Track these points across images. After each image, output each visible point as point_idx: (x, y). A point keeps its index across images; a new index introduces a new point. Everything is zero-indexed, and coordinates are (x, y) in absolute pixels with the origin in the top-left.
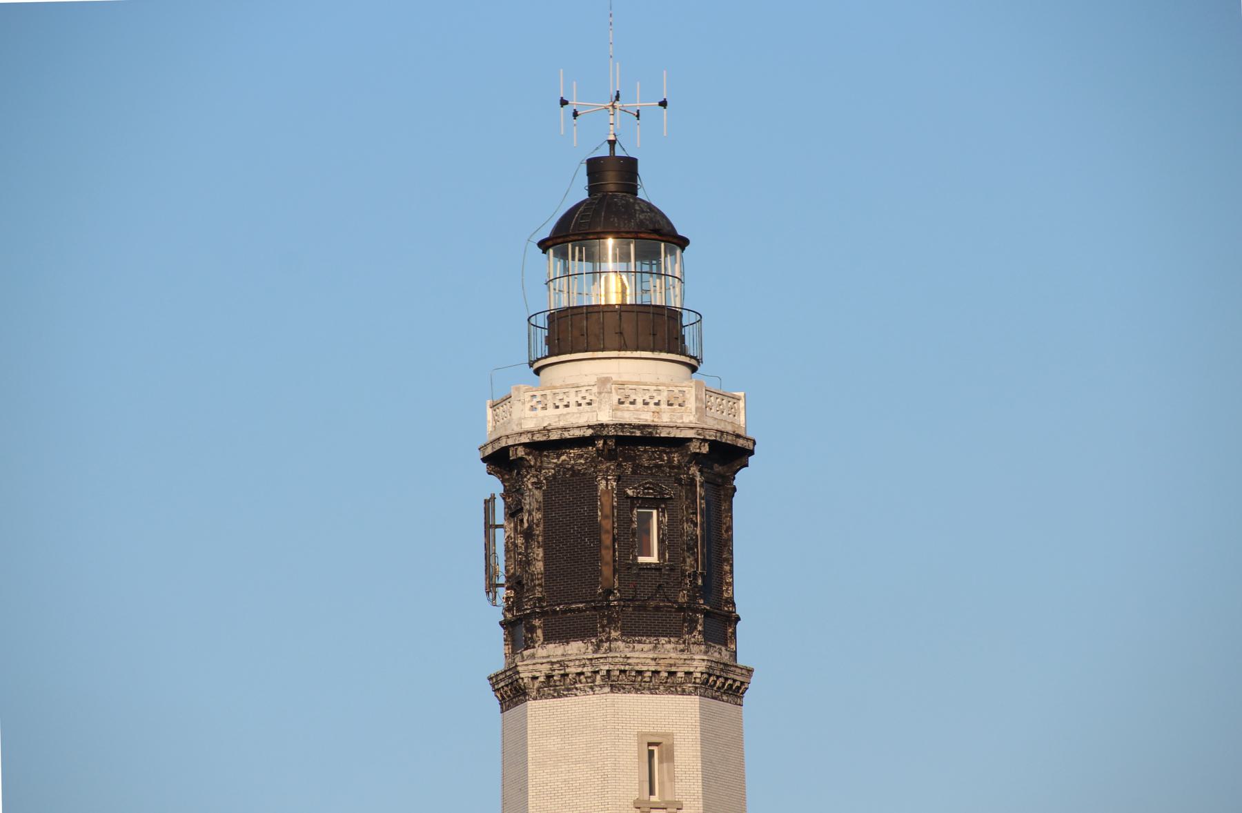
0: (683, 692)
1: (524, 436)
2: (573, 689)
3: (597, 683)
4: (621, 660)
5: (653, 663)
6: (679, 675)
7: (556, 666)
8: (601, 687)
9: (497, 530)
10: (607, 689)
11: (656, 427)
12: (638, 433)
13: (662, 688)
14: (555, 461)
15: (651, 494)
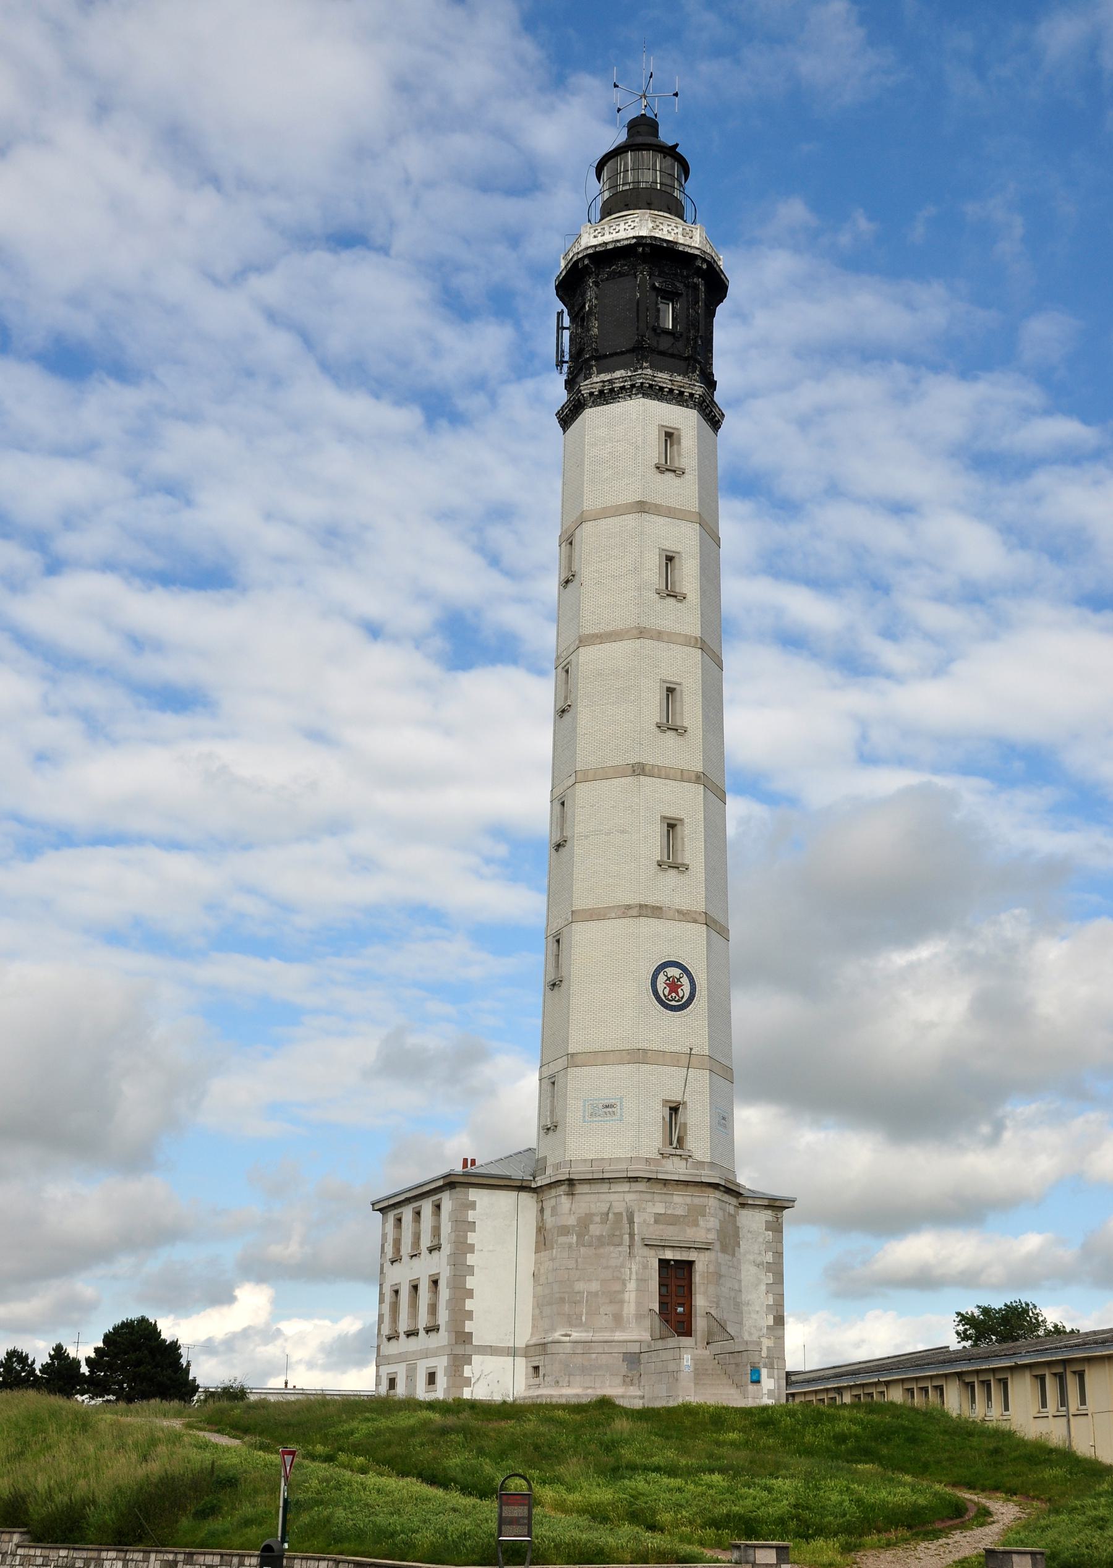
0: (687, 407)
1: (589, 250)
2: (616, 398)
3: (634, 393)
4: (650, 377)
6: (686, 394)
8: (636, 394)
9: (564, 331)
10: (641, 396)
11: (676, 243)
12: (665, 245)
13: (674, 401)
14: (608, 270)
15: (670, 288)
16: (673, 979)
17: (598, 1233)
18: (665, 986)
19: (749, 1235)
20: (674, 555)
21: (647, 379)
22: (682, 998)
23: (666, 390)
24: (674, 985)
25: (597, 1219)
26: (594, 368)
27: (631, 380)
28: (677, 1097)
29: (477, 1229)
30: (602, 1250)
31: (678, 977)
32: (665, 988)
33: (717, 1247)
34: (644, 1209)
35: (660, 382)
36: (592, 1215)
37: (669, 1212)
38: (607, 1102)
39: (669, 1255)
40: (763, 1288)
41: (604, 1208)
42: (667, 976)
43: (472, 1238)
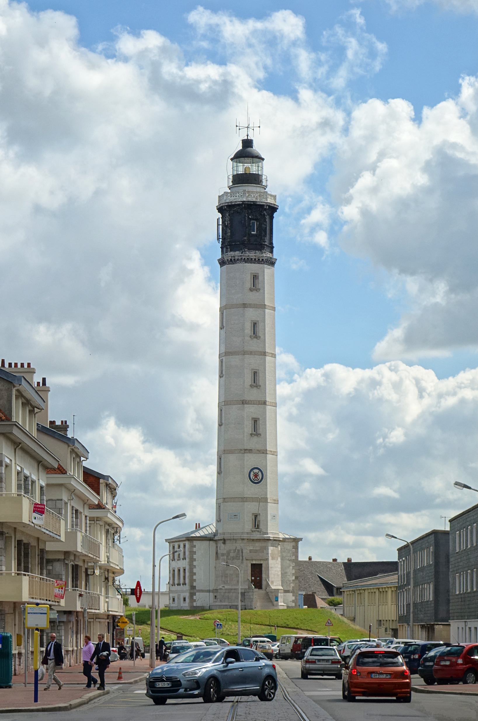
8: (243, 262)
10: (244, 262)
12: (252, 203)
17: (232, 556)
24: (256, 475)
25: (232, 551)
36: (231, 550)
37: (254, 549)
38: (235, 514)
39: (254, 562)
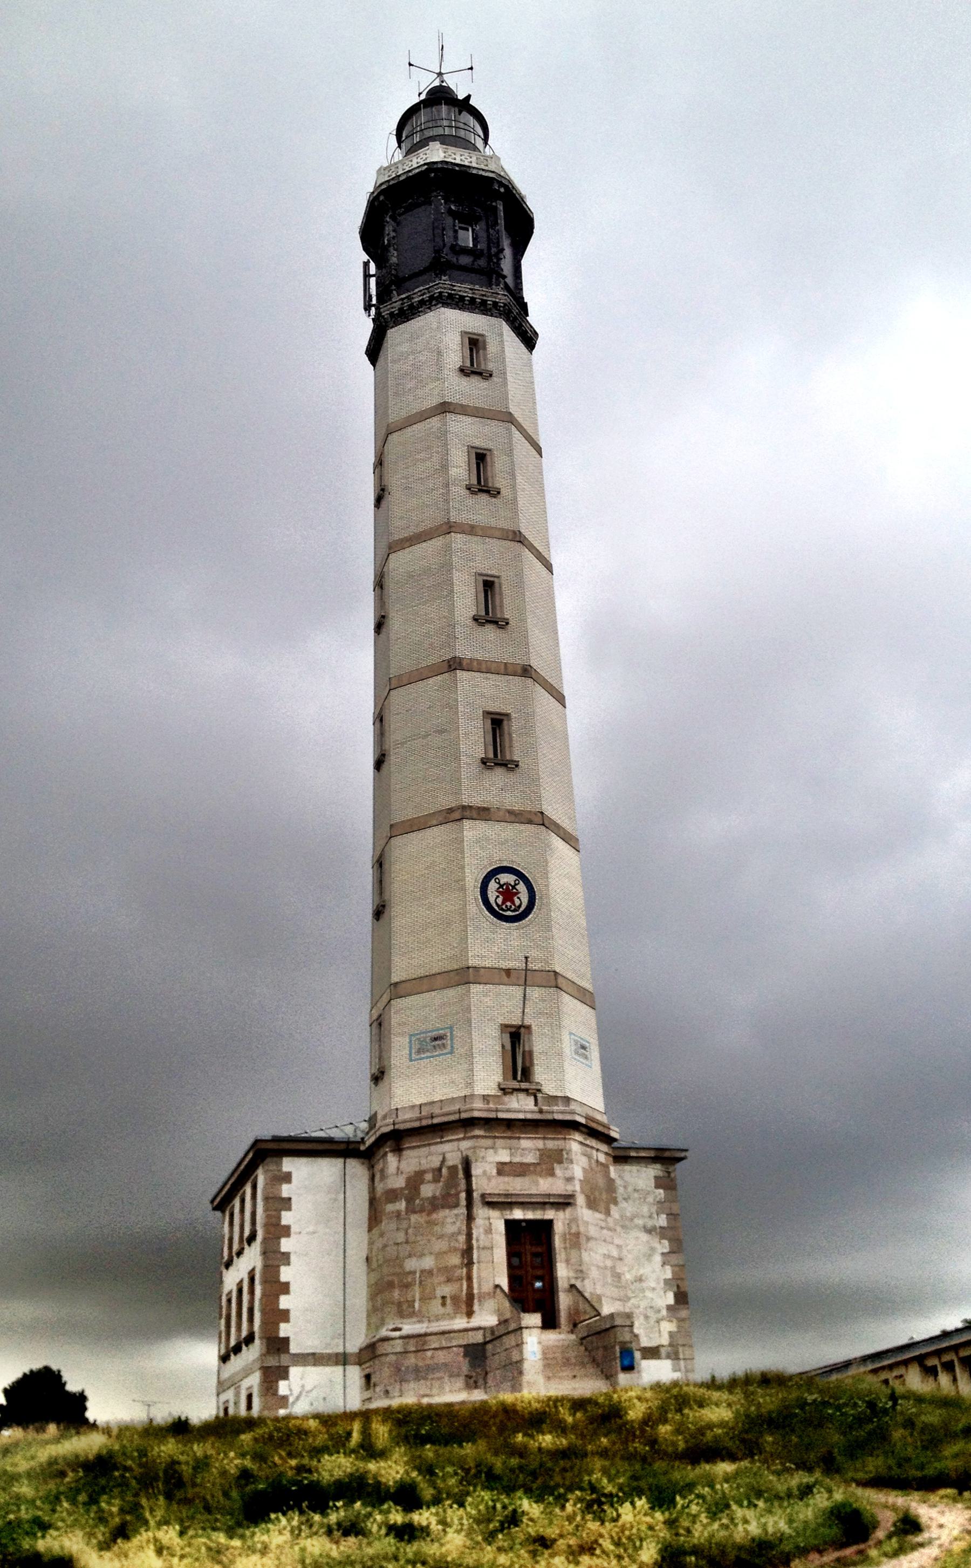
0: (492, 315)
5: (470, 292)
7: (405, 301)
8: (435, 305)
12: (457, 168)
16: (508, 888)
17: (430, 1195)
18: (497, 894)
19: (636, 1195)
20: (485, 452)
21: (445, 288)
22: (520, 906)
23: (467, 298)
24: (508, 893)
25: (429, 1177)
26: (394, 292)
27: (429, 292)
28: (516, 1021)
29: (294, 1206)
30: (434, 1216)
31: (513, 883)
32: (498, 897)
33: (581, 1200)
34: (483, 1158)
35: (460, 291)
36: (424, 1172)
37: (517, 1159)
38: (435, 1034)
40: (658, 1259)
41: (435, 1162)
42: (499, 883)
43: (287, 1218)
